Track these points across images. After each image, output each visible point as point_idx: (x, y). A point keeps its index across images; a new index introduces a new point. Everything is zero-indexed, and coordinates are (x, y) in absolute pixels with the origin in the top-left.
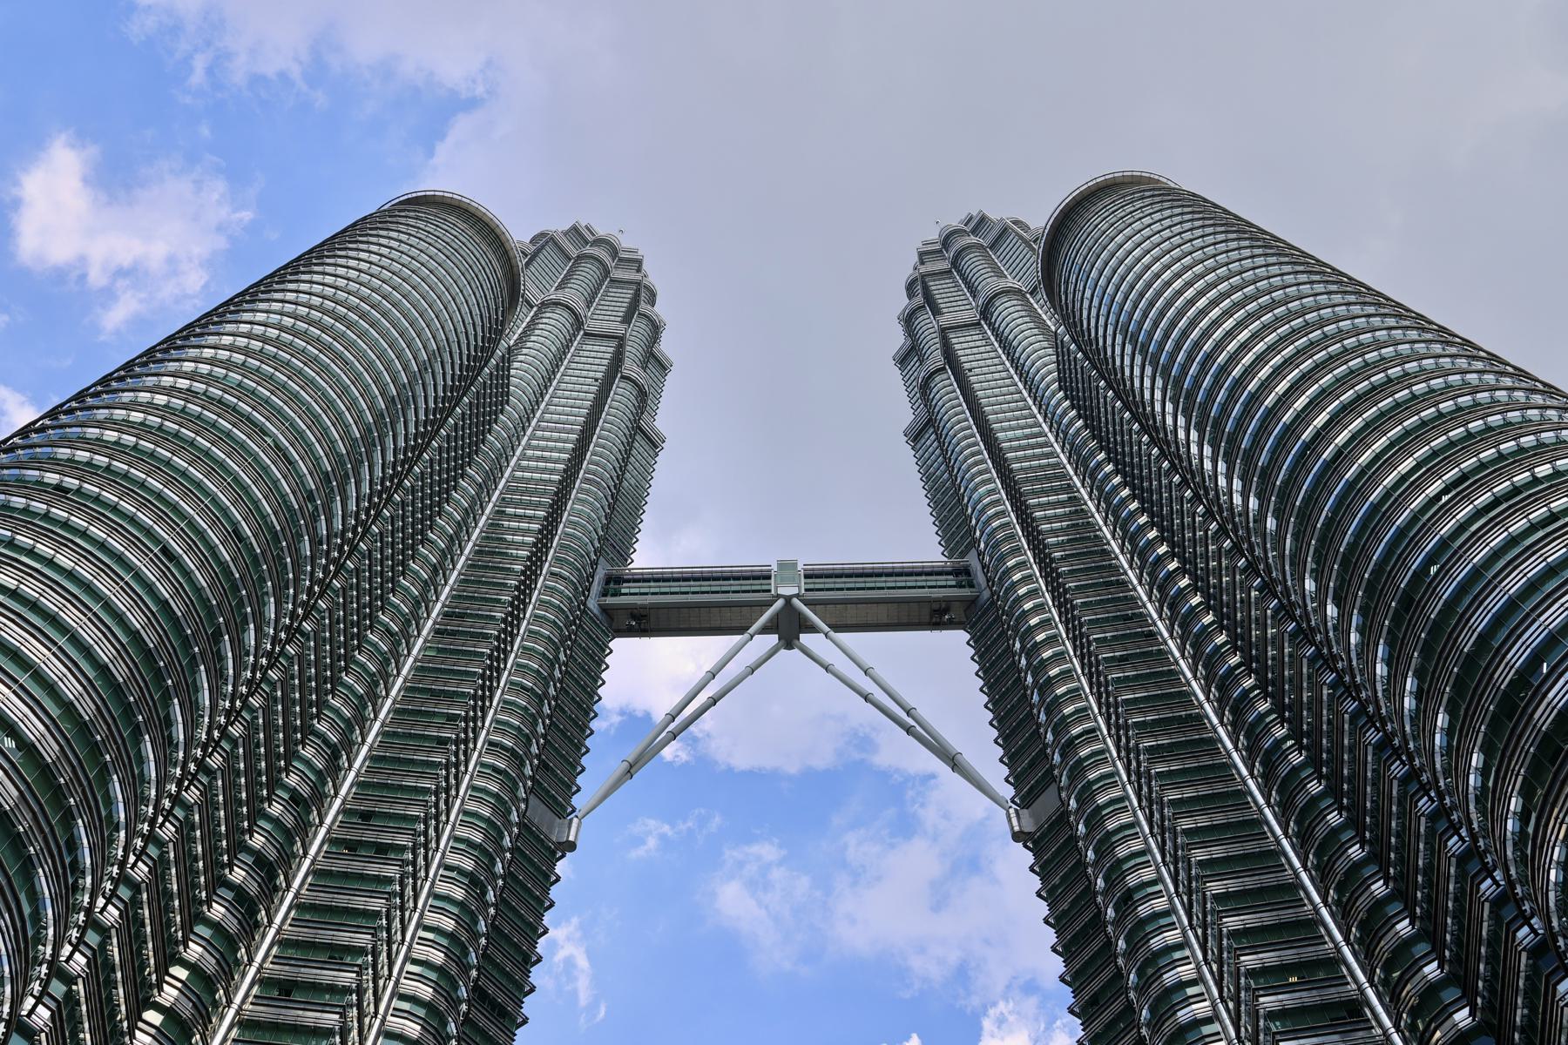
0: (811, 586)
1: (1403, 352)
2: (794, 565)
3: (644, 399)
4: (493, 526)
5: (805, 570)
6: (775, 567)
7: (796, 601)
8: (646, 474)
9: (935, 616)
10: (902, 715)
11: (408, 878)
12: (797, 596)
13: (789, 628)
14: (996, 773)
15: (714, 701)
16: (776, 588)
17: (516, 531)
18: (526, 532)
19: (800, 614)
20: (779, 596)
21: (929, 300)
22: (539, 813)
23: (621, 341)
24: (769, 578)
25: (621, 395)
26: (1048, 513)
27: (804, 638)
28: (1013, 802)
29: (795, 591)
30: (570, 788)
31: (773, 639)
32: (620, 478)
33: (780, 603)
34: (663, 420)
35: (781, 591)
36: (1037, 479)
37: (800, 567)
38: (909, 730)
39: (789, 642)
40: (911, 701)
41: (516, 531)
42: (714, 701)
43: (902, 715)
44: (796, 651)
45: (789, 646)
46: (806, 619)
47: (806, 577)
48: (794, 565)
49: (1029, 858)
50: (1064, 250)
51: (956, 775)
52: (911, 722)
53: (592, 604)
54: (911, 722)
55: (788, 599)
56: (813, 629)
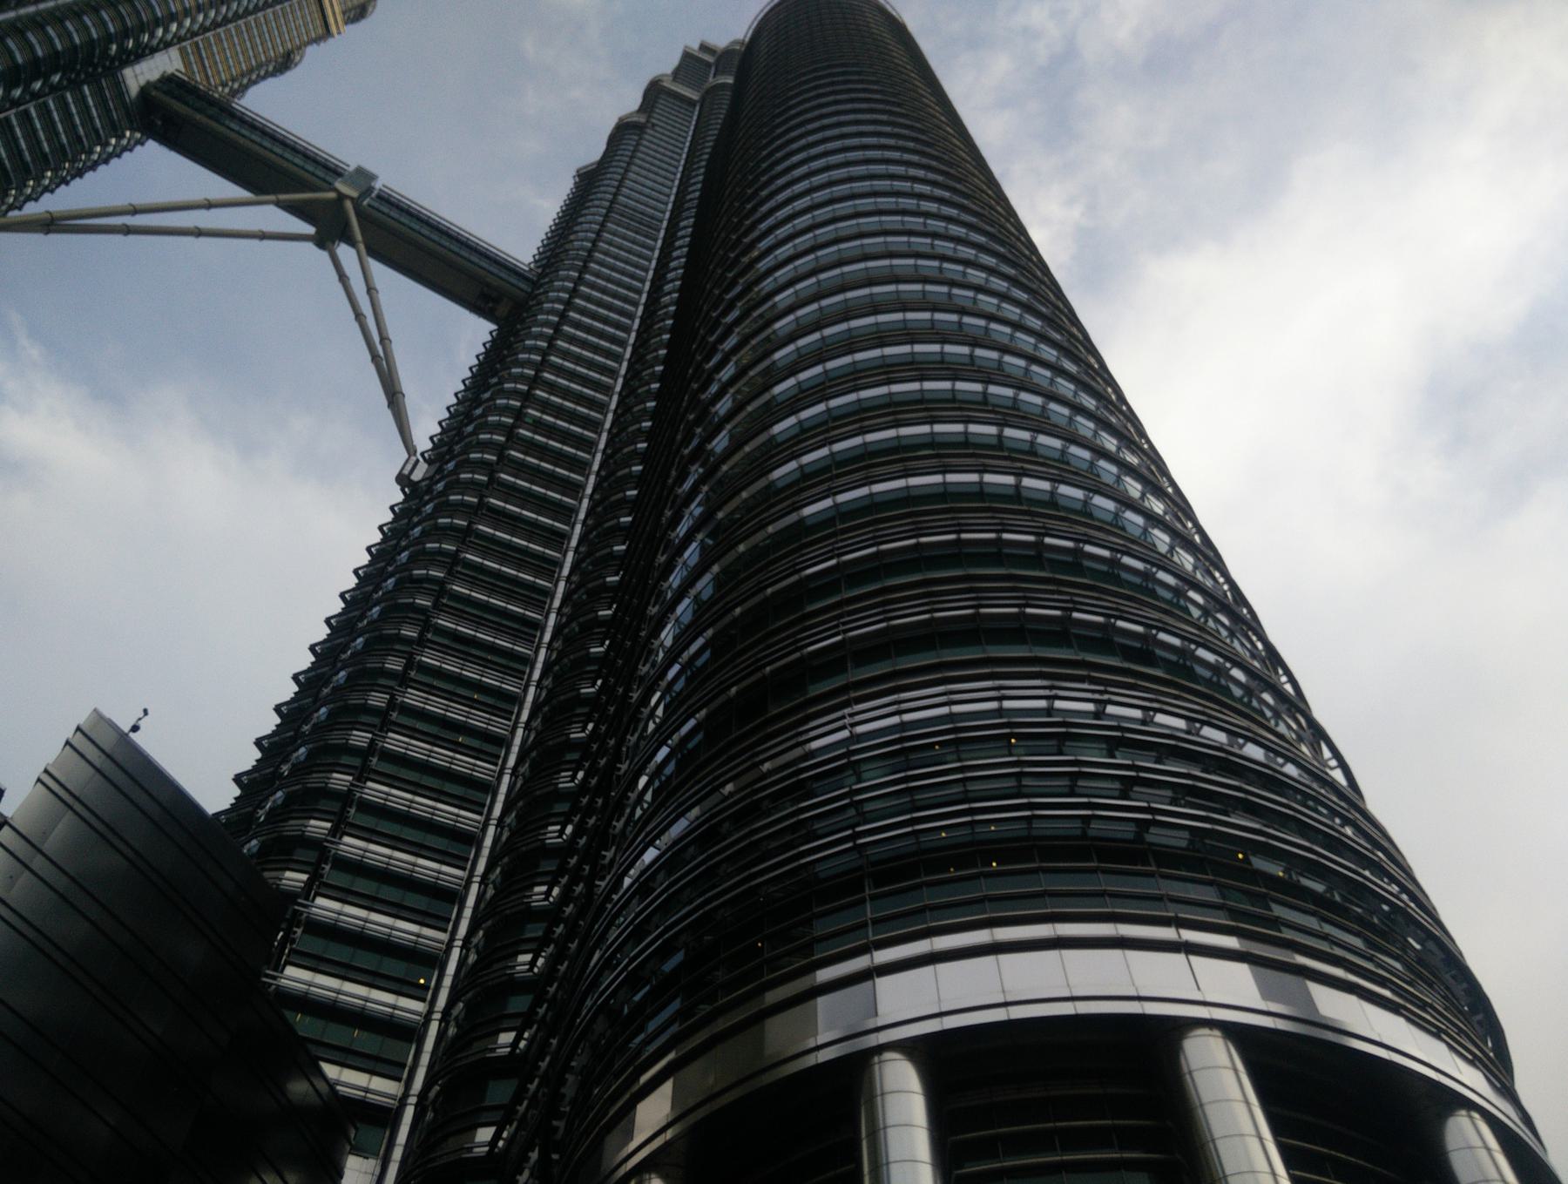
1: (1073, 461)
2: (373, 177)
5: (380, 190)
7: (349, 205)
10: (376, 339)
12: (352, 199)
31: (310, 230)
33: (332, 195)
38: (375, 358)
39: (323, 240)
40: (392, 333)
43: (376, 339)
44: (324, 255)
46: (347, 224)
55: (342, 197)
56: (352, 242)
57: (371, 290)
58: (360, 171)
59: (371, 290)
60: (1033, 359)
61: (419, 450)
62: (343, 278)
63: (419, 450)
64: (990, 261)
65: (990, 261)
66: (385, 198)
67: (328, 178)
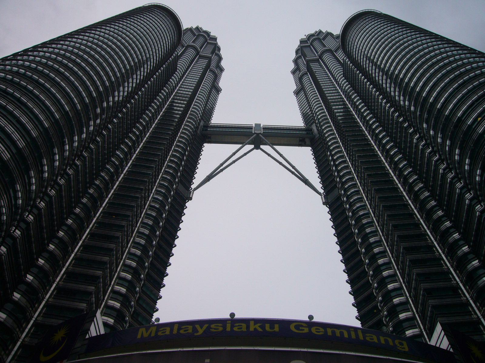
0: (265, 131)
2: (260, 125)
3: (216, 77)
6: (254, 126)
7: (260, 135)
8: (216, 100)
9: (301, 143)
11: (139, 207)
12: (260, 133)
13: (257, 143)
14: (319, 186)
15: (234, 162)
16: (254, 131)
17: (176, 110)
19: (261, 138)
20: (255, 133)
21: (305, 56)
22: (181, 188)
23: (210, 59)
24: (252, 128)
25: (209, 76)
26: (338, 111)
27: (262, 147)
28: (323, 194)
29: (260, 132)
30: (190, 182)
31: (252, 146)
32: (206, 105)
34: (222, 83)
35: (256, 132)
36: (335, 102)
37: (262, 126)
38: (293, 173)
39: (257, 147)
41: (176, 110)
42: (234, 162)
44: (259, 150)
45: (257, 149)
47: (263, 129)
48: (260, 125)
49: (328, 210)
50: (349, 30)
51: (307, 186)
52: (293, 170)
53: (198, 132)
54: (293, 170)
55: (258, 134)
57: (281, 155)
58: (256, 125)
59: (281, 155)
60: (421, 41)
61: (322, 193)
62: (269, 155)
63: (322, 193)
64: (405, 29)
65: (405, 29)
66: (265, 128)
67: (251, 131)
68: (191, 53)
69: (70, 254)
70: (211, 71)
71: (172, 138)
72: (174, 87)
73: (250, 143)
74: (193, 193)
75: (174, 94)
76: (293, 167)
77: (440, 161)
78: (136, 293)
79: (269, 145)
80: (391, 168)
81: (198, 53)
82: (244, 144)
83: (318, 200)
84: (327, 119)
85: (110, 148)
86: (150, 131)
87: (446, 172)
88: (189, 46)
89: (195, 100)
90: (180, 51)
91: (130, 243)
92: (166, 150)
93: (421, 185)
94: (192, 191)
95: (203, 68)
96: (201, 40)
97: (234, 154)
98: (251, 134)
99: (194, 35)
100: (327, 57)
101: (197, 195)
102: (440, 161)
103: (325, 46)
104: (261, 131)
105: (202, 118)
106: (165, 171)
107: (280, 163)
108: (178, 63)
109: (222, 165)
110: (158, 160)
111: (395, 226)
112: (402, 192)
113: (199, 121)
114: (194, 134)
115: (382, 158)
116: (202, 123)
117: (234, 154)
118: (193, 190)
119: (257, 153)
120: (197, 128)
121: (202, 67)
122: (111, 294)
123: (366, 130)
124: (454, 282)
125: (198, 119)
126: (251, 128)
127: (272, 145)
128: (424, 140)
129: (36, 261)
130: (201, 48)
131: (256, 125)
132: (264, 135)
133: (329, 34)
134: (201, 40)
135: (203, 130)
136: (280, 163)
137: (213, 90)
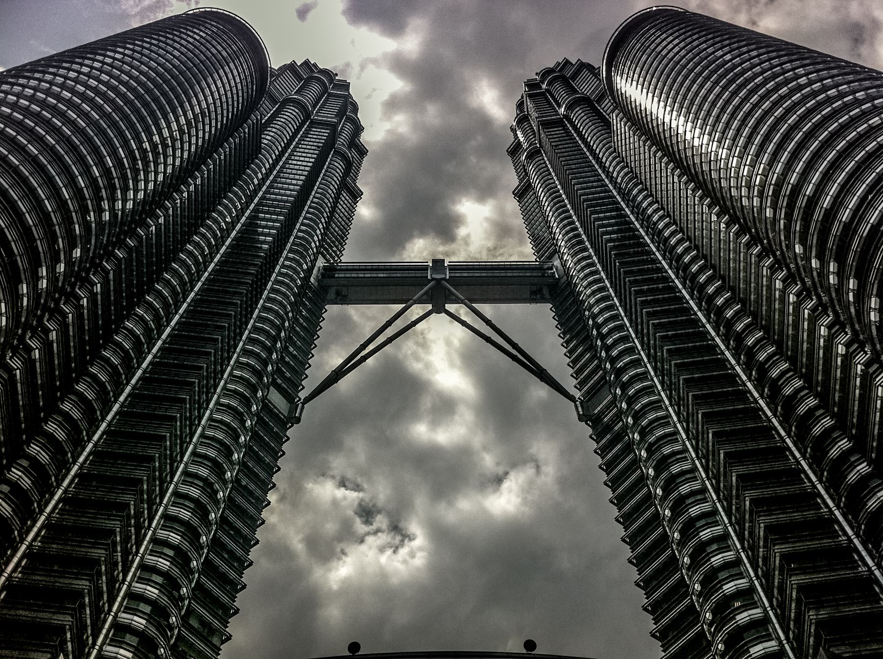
0: (453, 275)
4: (253, 217)
12: (444, 279)
14: (570, 384)
15: (390, 340)
16: (431, 275)
17: (263, 234)
18: (268, 235)
20: (433, 279)
23: (333, 127)
27: (448, 307)
39: (439, 309)
41: (263, 234)
42: (390, 340)
47: (449, 270)
49: (590, 431)
53: (312, 280)
55: (438, 281)
57: (488, 322)
58: (434, 261)
59: (488, 322)
66: (453, 268)
67: (424, 275)
68: (291, 112)
69: (112, 405)
70: (338, 153)
71: (257, 281)
72: (257, 187)
73: (420, 301)
74: (303, 408)
75: (256, 201)
76: (515, 346)
77: (837, 327)
78: (182, 598)
79: (462, 302)
80: (728, 348)
81: (307, 115)
82: (408, 302)
83: (571, 411)
84: (582, 242)
85: (170, 245)
86: (203, 279)
87: (851, 350)
88: (287, 101)
89: (300, 221)
90: (267, 109)
91: (168, 495)
92: (238, 323)
93: (798, 383)
94: (300, 405)
95: (318, 147)
96: (315, 89)
97: (389, 323)
98: (424, 281)
99: (299, 78)
100: (579, 116)
101: (309, 413)
102: (837, 327)
103: (575, 91)
104: (446, 275)
105: (319, 253)
106: (254, 326)
107: (488, 340)
108: (263, 136)
109: (364, 346)
110: (239, 302)
111: (733, 458)
112: (743, 382)
113: (312, 257)
114: (302, 285)
115: (717, 339)
116: (321, 262)
117: (389, 323)
118: (302, 401)
119: (439, 321)
120: (310, 271)
121: (315, 144)
122: (139, 572)
123: (677, 277)
124: (825, 510)
125: (310, 252)
126: (425, 269)
127: (469, 301)
128: (814, 297)
129: (25, 447)
130: (314, 107)
131: (434, 261)
132: (452, 281)
133: (584, 66)
134: (315, 89)
135: (323, 275)
136: (488, 340)
137: (345, 195)
